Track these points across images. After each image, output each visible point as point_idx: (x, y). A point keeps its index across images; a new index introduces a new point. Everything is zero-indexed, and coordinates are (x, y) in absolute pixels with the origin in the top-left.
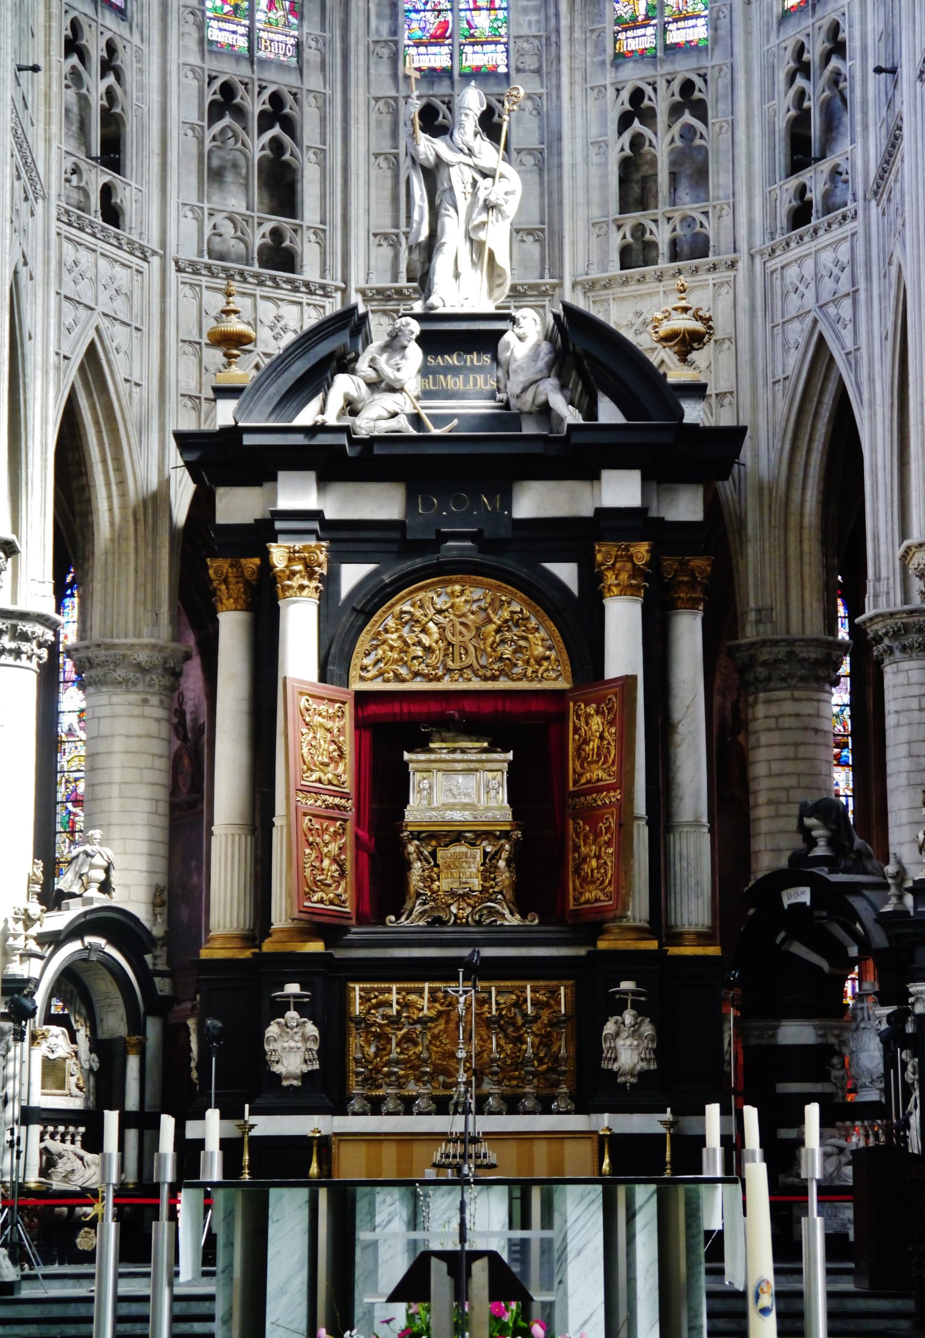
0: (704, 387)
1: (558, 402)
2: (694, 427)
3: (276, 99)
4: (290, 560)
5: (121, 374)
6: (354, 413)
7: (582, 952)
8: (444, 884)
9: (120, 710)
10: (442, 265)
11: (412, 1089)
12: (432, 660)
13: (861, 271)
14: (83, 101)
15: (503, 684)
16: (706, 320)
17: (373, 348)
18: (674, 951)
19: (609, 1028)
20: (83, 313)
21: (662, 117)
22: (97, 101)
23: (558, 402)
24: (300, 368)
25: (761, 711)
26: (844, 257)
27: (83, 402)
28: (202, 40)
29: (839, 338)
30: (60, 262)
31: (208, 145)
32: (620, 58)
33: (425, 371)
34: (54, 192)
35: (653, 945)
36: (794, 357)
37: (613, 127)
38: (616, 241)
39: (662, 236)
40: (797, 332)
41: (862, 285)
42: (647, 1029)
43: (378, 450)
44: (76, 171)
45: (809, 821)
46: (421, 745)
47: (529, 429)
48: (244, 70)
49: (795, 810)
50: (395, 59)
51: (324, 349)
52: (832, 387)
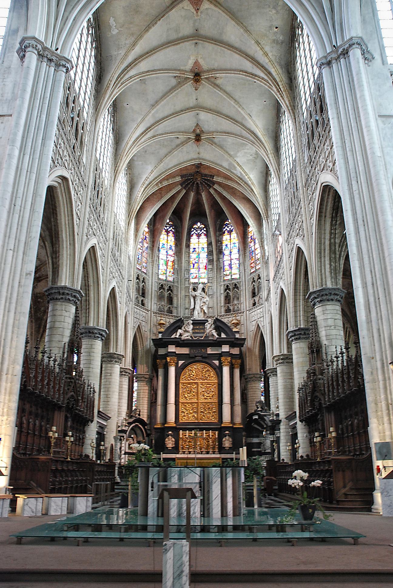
0: (239, 332)
2: (237, 338)
3: (170, 287)
4: (170, 360)
5: (144, 330)
6: (182, 336)
7: (219, 427)
9: (142, 385)
10: (196, 313)
12: (194, 377)
13: (264, 313)
14: (139, 287)
17: (184, 326)
18: (235, 426)
19: (224, 439)
20: (138, 320)
21: (231, 290)
22: (141, 287)
23: (215, 334)
24: (173, 328)
25: (249, 386)
26: (262, 311)
27: (137, 334)
28: (158, 278)
29: (261, 324)
30: (134, 312)
31: (159, 294)
34: (133, 300)
35: (231, 425)
36: (254, 327)
40: (254, 323)
41: (264, 315)
42: (231, 440)
43: (185, 342)
44: (137, 298)
45: (257, 404)
48: (165, 282)
49: (255, 402)
50: (189, 280)
51: (178, 324)
52: (260, 332)
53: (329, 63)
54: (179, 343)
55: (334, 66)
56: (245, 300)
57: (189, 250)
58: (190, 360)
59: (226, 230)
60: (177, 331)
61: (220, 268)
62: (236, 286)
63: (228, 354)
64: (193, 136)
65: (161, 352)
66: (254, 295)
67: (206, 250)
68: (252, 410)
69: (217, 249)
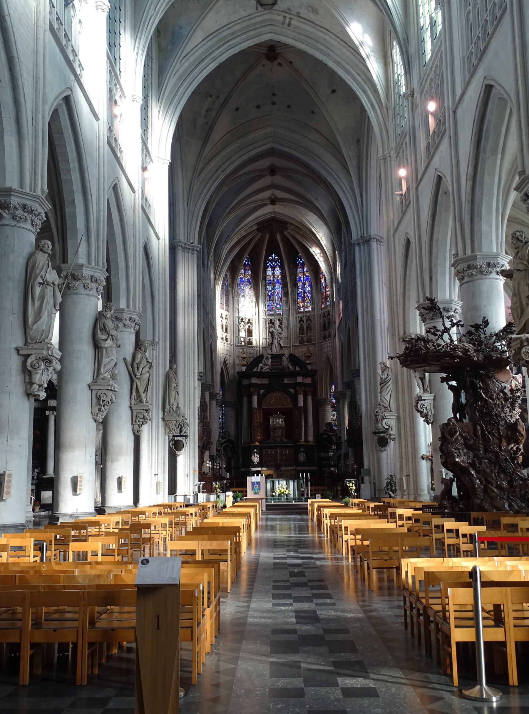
1: (290, 367)
3: (249, 320)
8: (276, 435)
11: (272, 464)
15: (283, 407)
16: (311, 354)
17: (264, 359)
21: (305, 321)
22: (224, 324)
23: (290, 367)
32: (299, 313)
33: (272, 362)
37: (298, 323)
38: (298, 339)
39: (305, 339)
46: (272, 415)
47: (287, 370)
53: (359, 244)
54: (260, 375)
55: (362, 247)
57: (265, 282)
58: (270, 389)
59: (300, 262)
60: (258, 366)
63: (302, 384)
64: (268, 202)
65: (245, 382)
67: (281, 281)
68: (321, 431)
69: (291, 282)
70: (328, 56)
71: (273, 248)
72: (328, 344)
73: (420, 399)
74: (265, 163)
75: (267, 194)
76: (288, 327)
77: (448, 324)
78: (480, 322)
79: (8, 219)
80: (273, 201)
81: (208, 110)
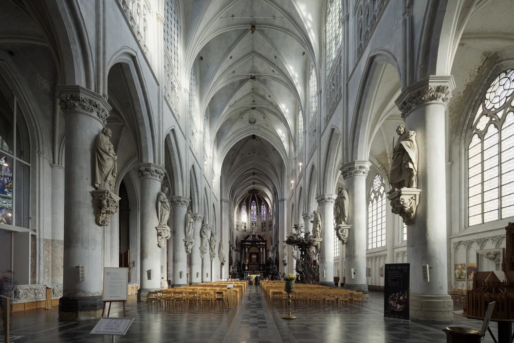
56: (267, 228)
58: (251, 246)
61: (260, 217)
62: (265, 223)
63: (262, 245)
65: (244, 244)
66: (270, 226)
70: (271, 141)
71: (253, 199)
72: (271, 232)
73: (293, 252)
74: (251, 171)
75: (252, 181)
76: (258, 226)
77: (300, 232)
78: (308, 232)
79: (180, 204)
80: (254, 184)
81: (233, 155)
